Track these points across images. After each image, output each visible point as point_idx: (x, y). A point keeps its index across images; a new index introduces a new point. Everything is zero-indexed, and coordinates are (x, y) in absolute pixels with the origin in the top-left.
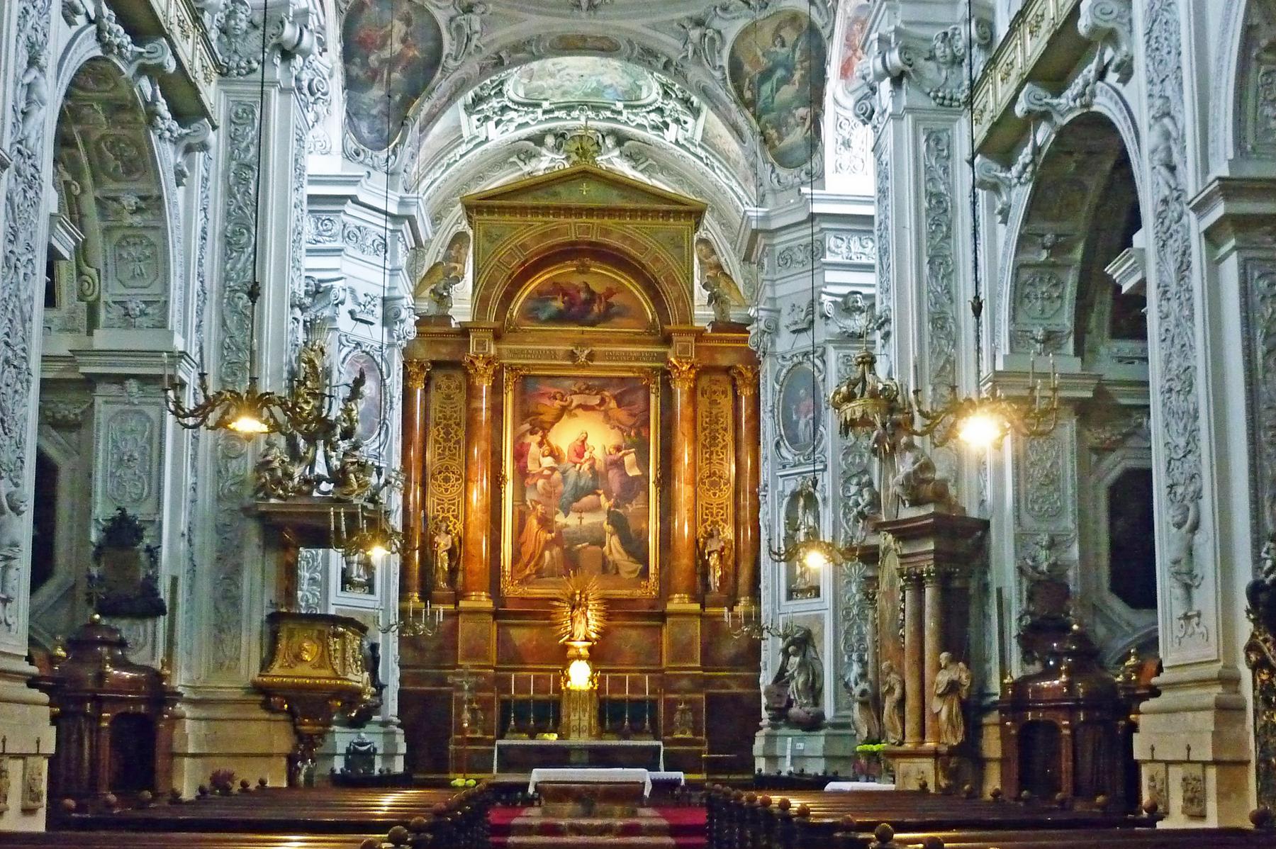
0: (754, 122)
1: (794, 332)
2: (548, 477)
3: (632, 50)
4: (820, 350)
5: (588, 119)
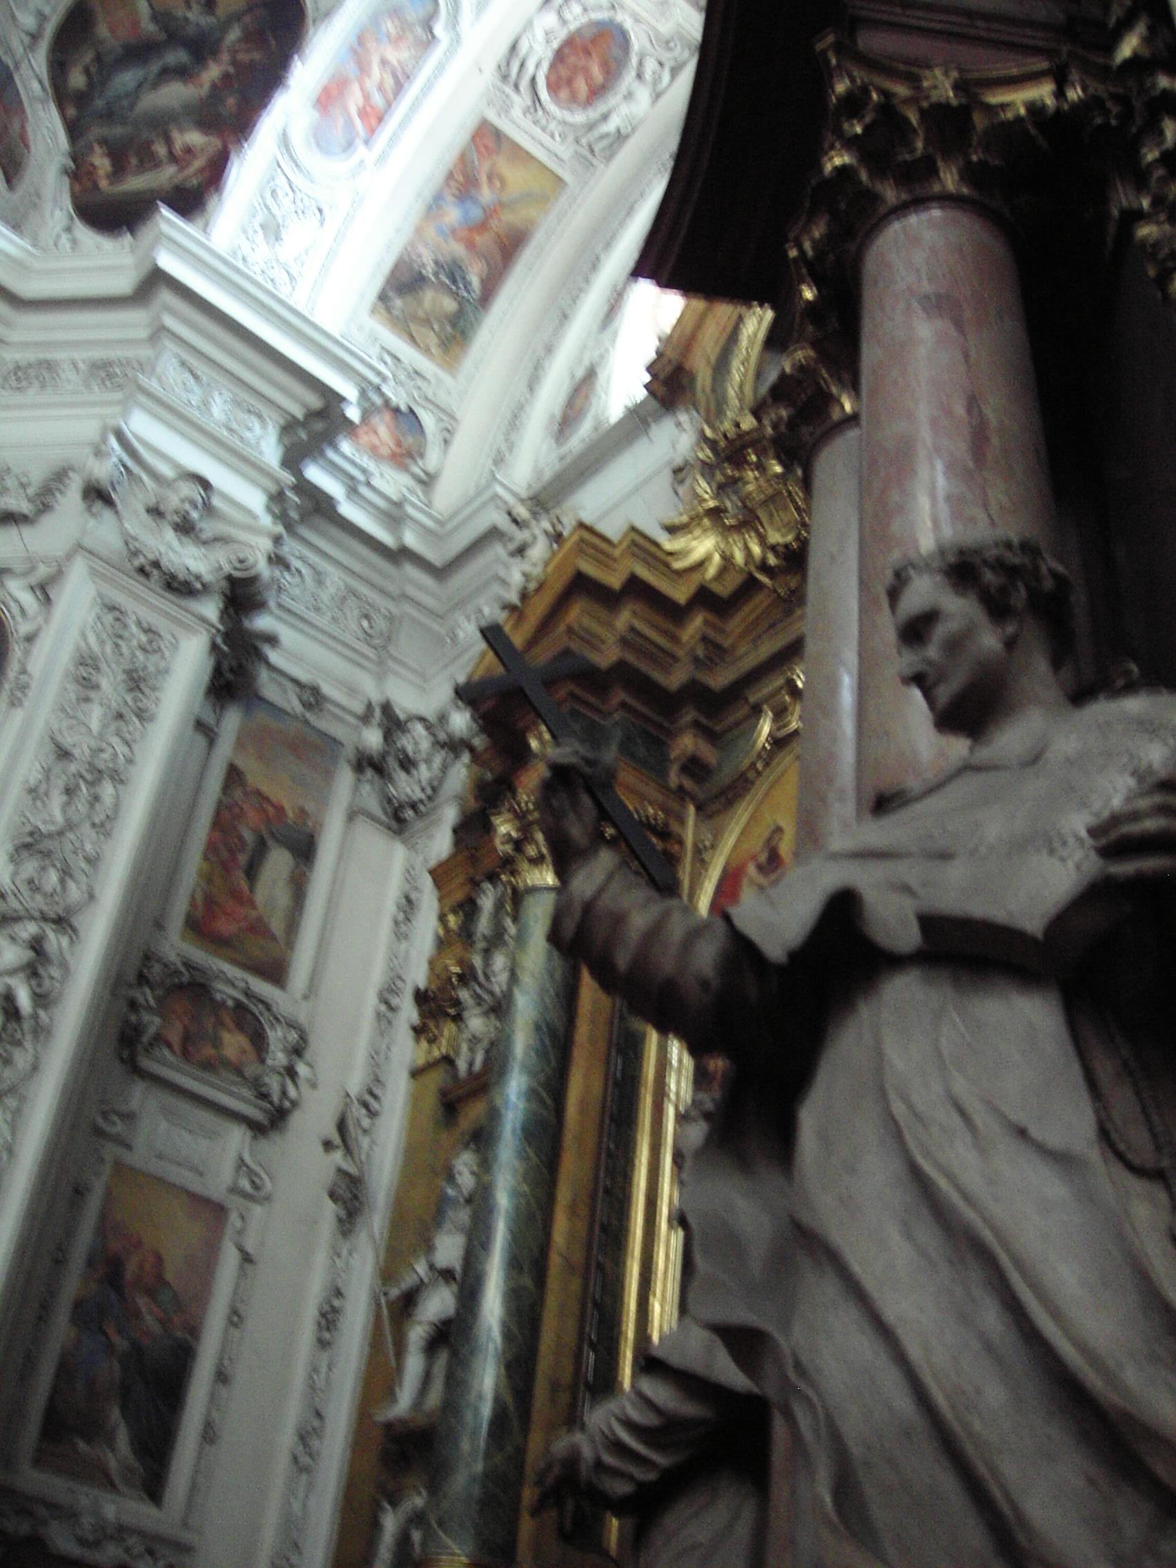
4: (43, 571)
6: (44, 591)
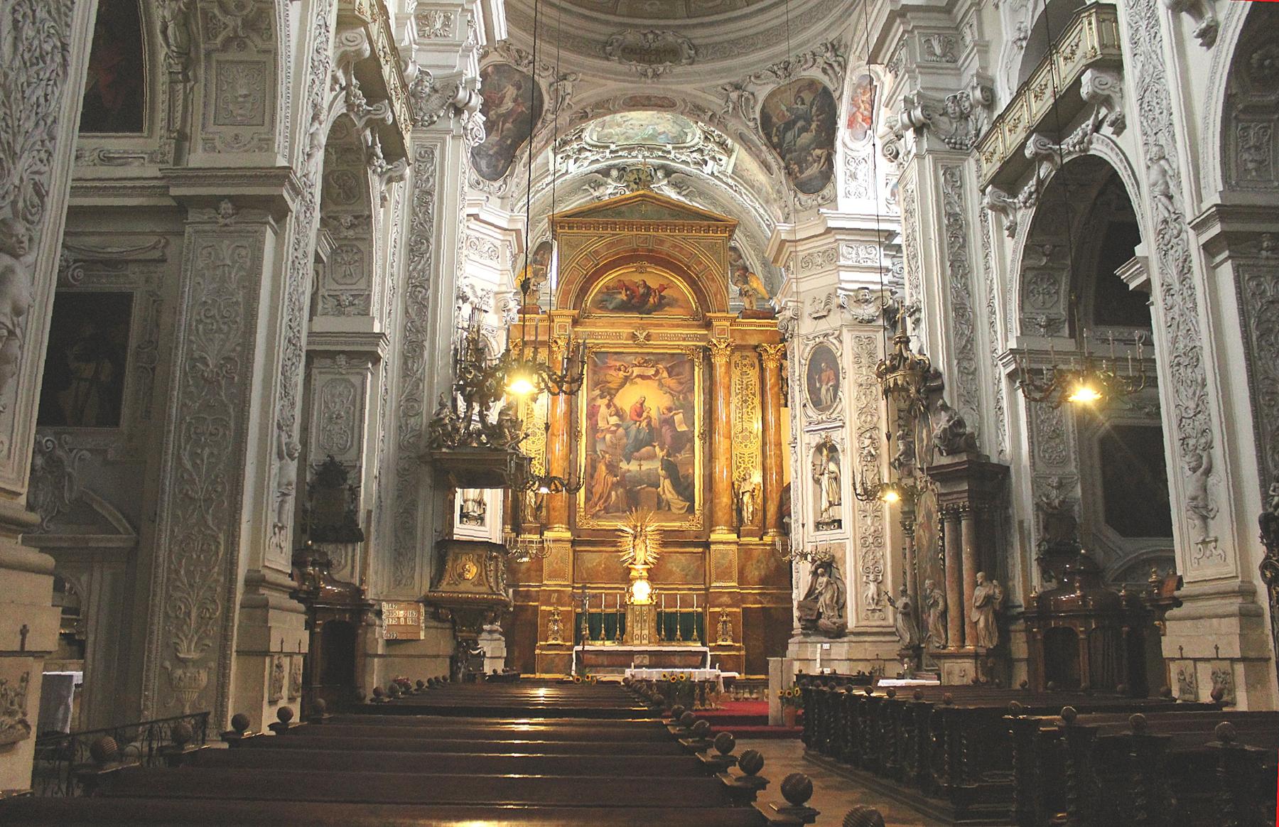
0: (780, 160)
1: (815, 318)
2: (614, 432)
3: (686, 106)
4: (837, 333)
5: (644, 157)
6: (838, 338)
